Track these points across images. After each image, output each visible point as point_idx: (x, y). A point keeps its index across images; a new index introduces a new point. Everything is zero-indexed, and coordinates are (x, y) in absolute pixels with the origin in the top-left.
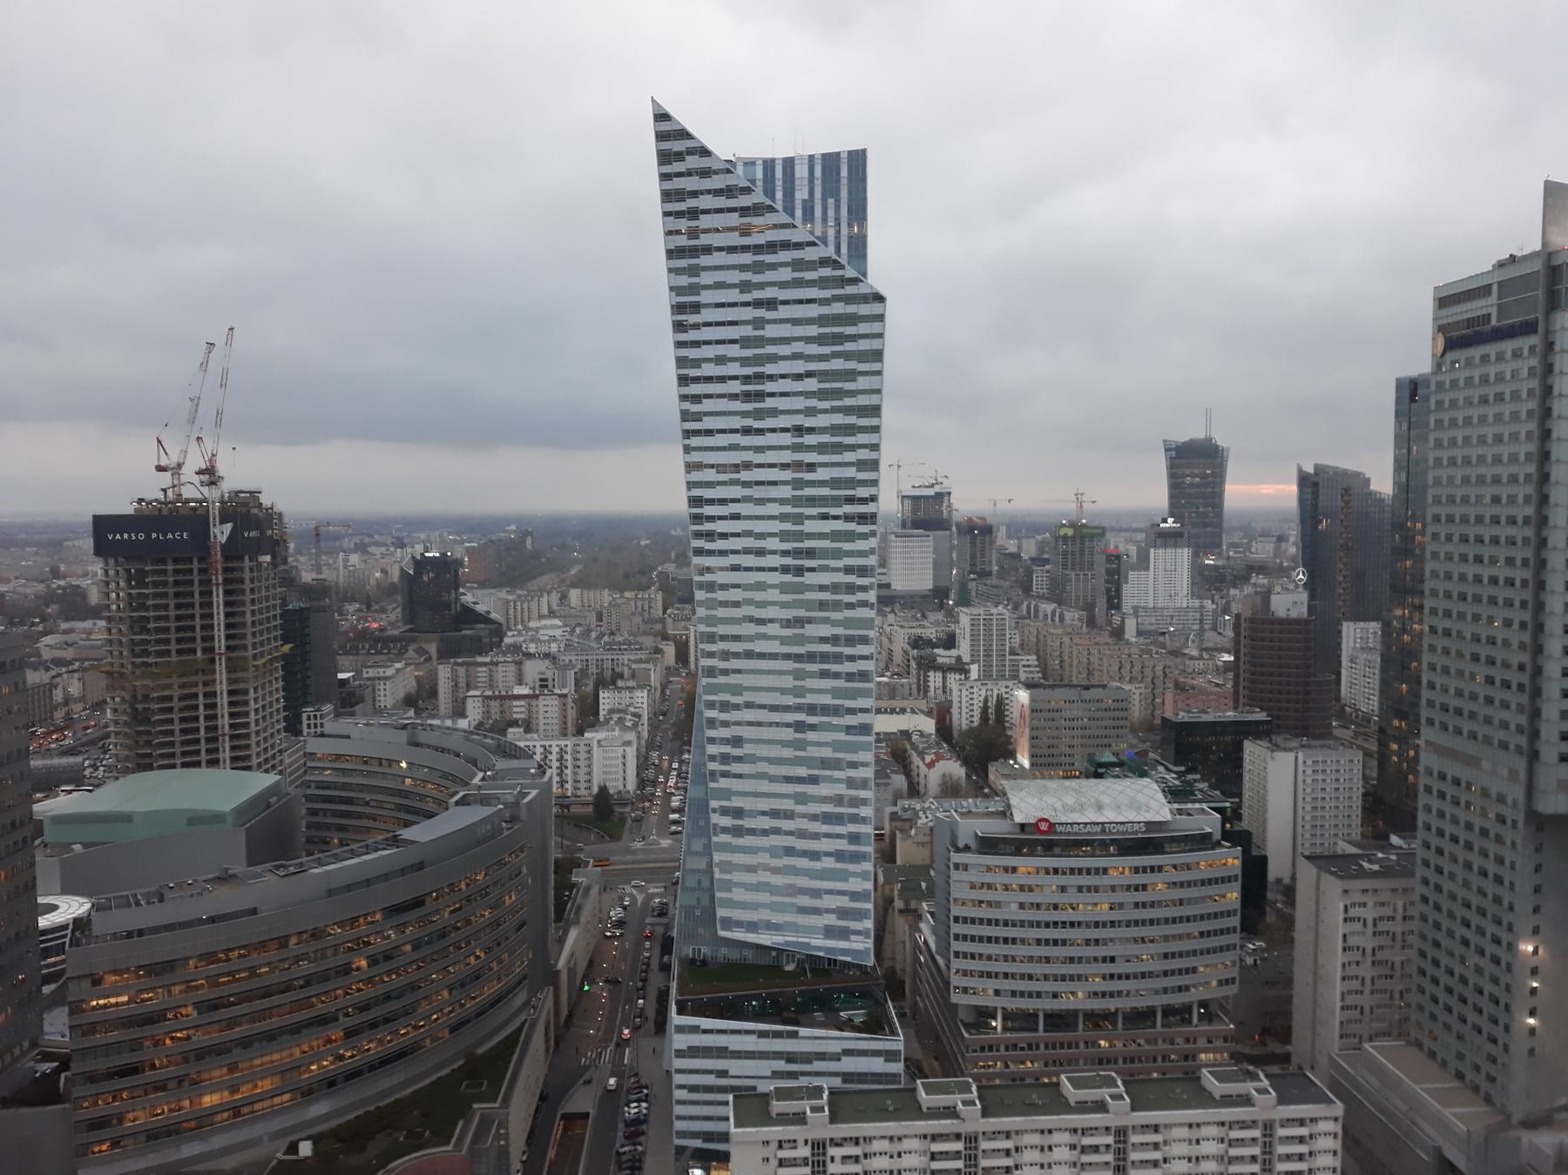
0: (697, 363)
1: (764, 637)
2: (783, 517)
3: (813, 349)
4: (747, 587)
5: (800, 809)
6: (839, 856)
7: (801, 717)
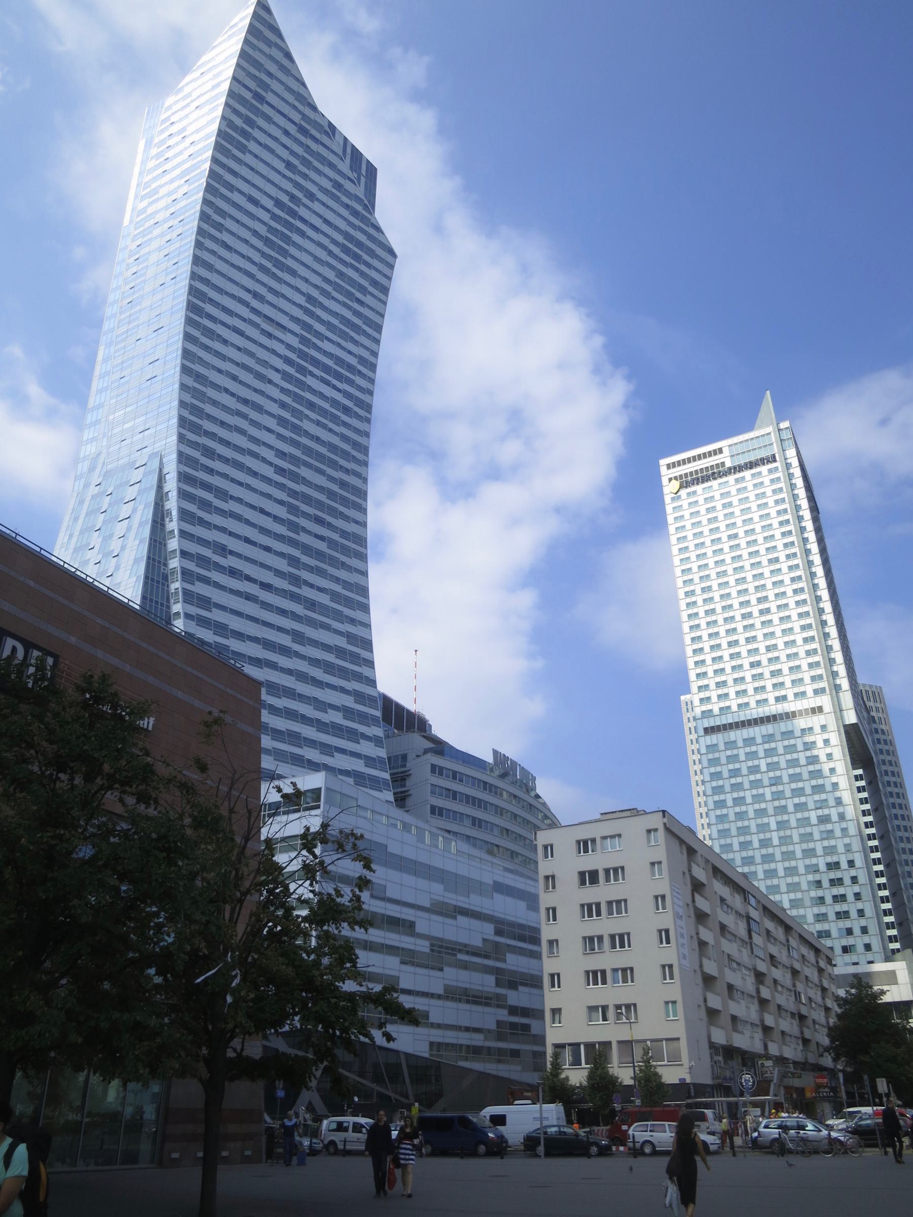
0: (231, 188)
1: (255, 455)
2: (288, 361)
3: (336, 250)
4: (246, 402)
5: (296, 647)
6: (348, 713)
7: (296, 553)
